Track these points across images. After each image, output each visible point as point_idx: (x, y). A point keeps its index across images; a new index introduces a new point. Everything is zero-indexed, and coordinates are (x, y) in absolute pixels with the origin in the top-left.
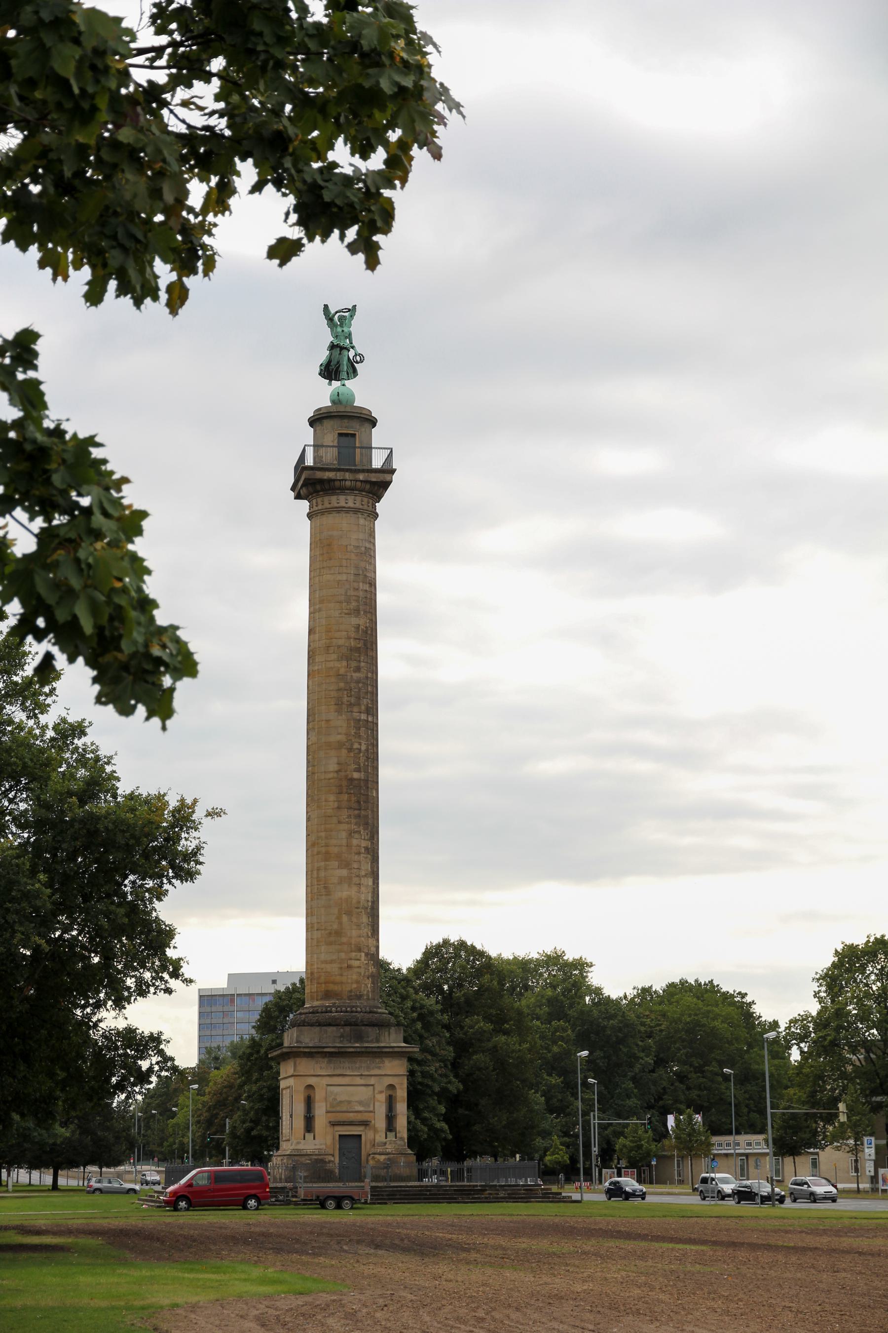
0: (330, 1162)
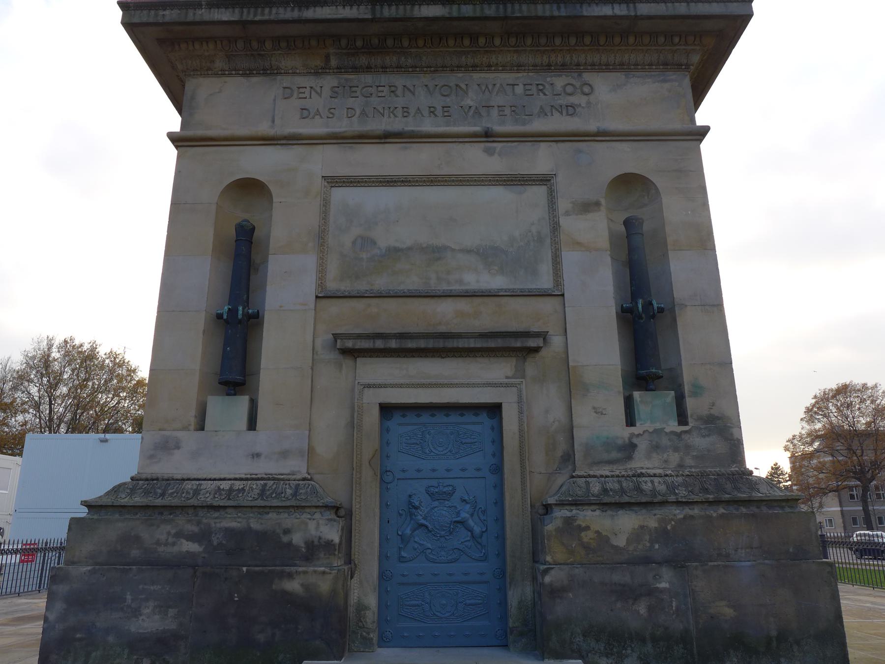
0: (315, 550)
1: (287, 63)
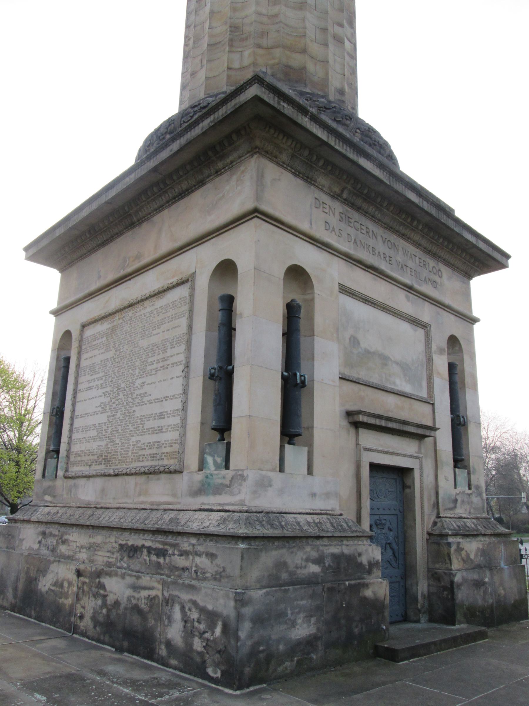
1: (323, 180)
